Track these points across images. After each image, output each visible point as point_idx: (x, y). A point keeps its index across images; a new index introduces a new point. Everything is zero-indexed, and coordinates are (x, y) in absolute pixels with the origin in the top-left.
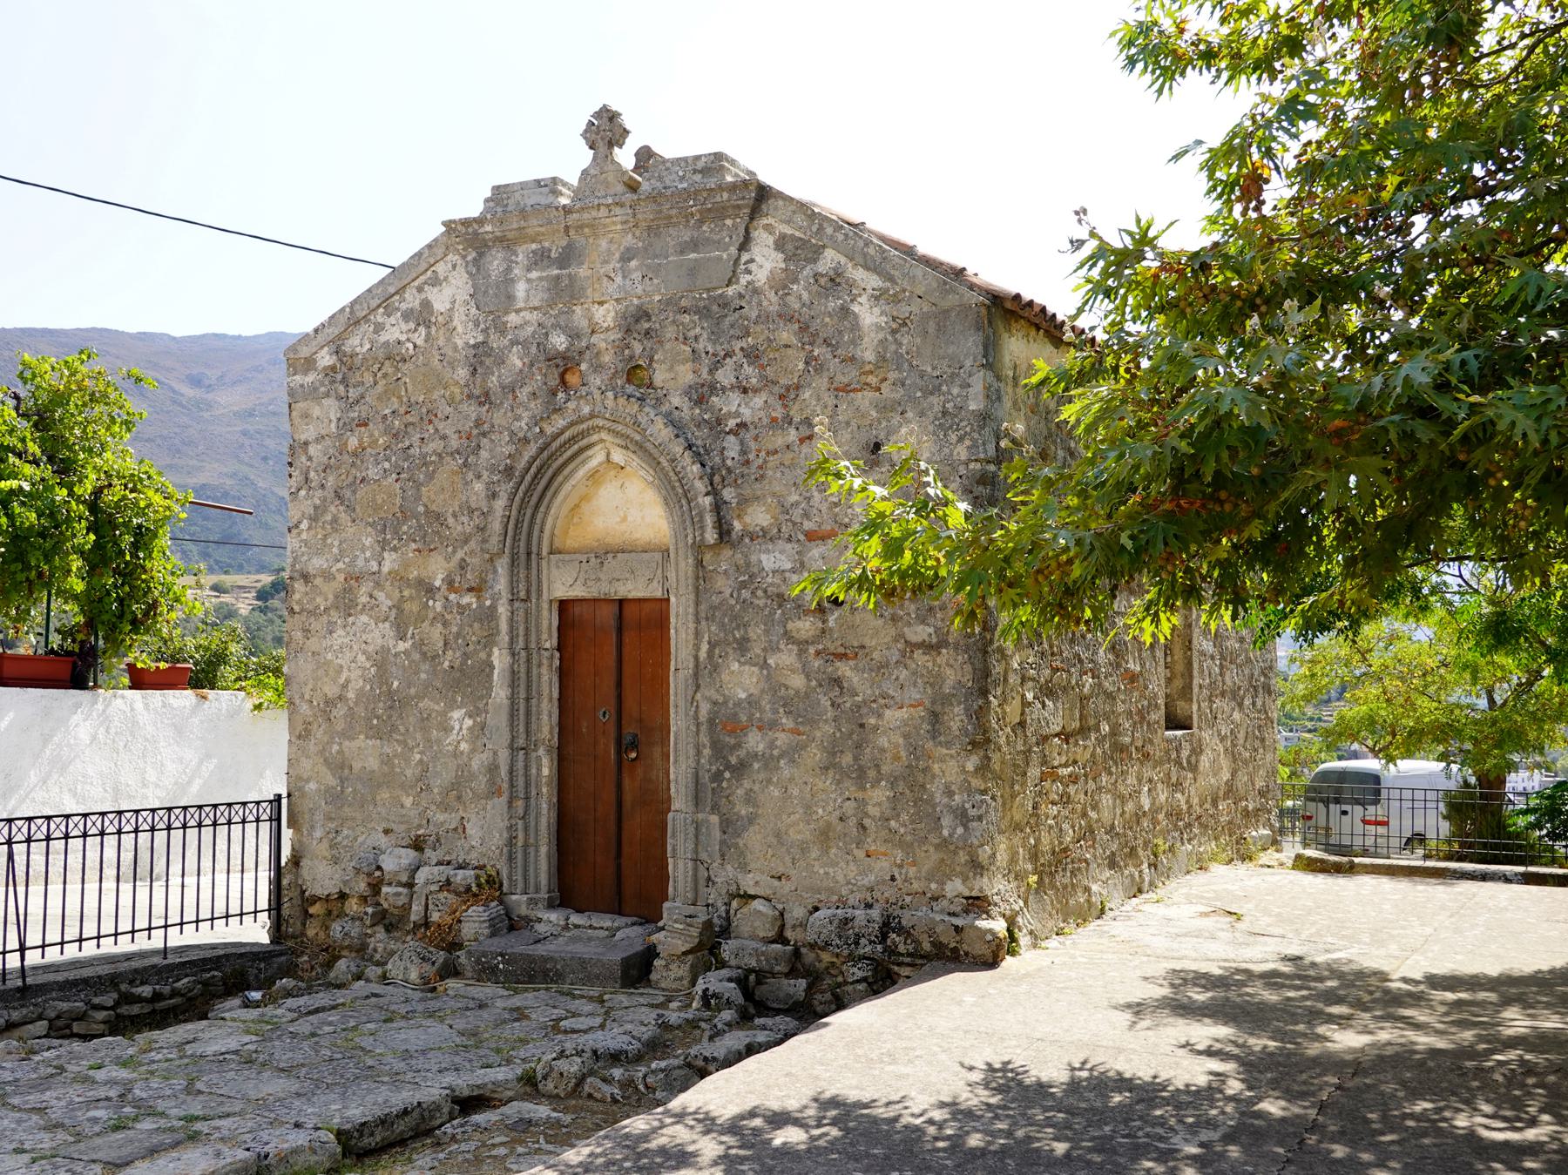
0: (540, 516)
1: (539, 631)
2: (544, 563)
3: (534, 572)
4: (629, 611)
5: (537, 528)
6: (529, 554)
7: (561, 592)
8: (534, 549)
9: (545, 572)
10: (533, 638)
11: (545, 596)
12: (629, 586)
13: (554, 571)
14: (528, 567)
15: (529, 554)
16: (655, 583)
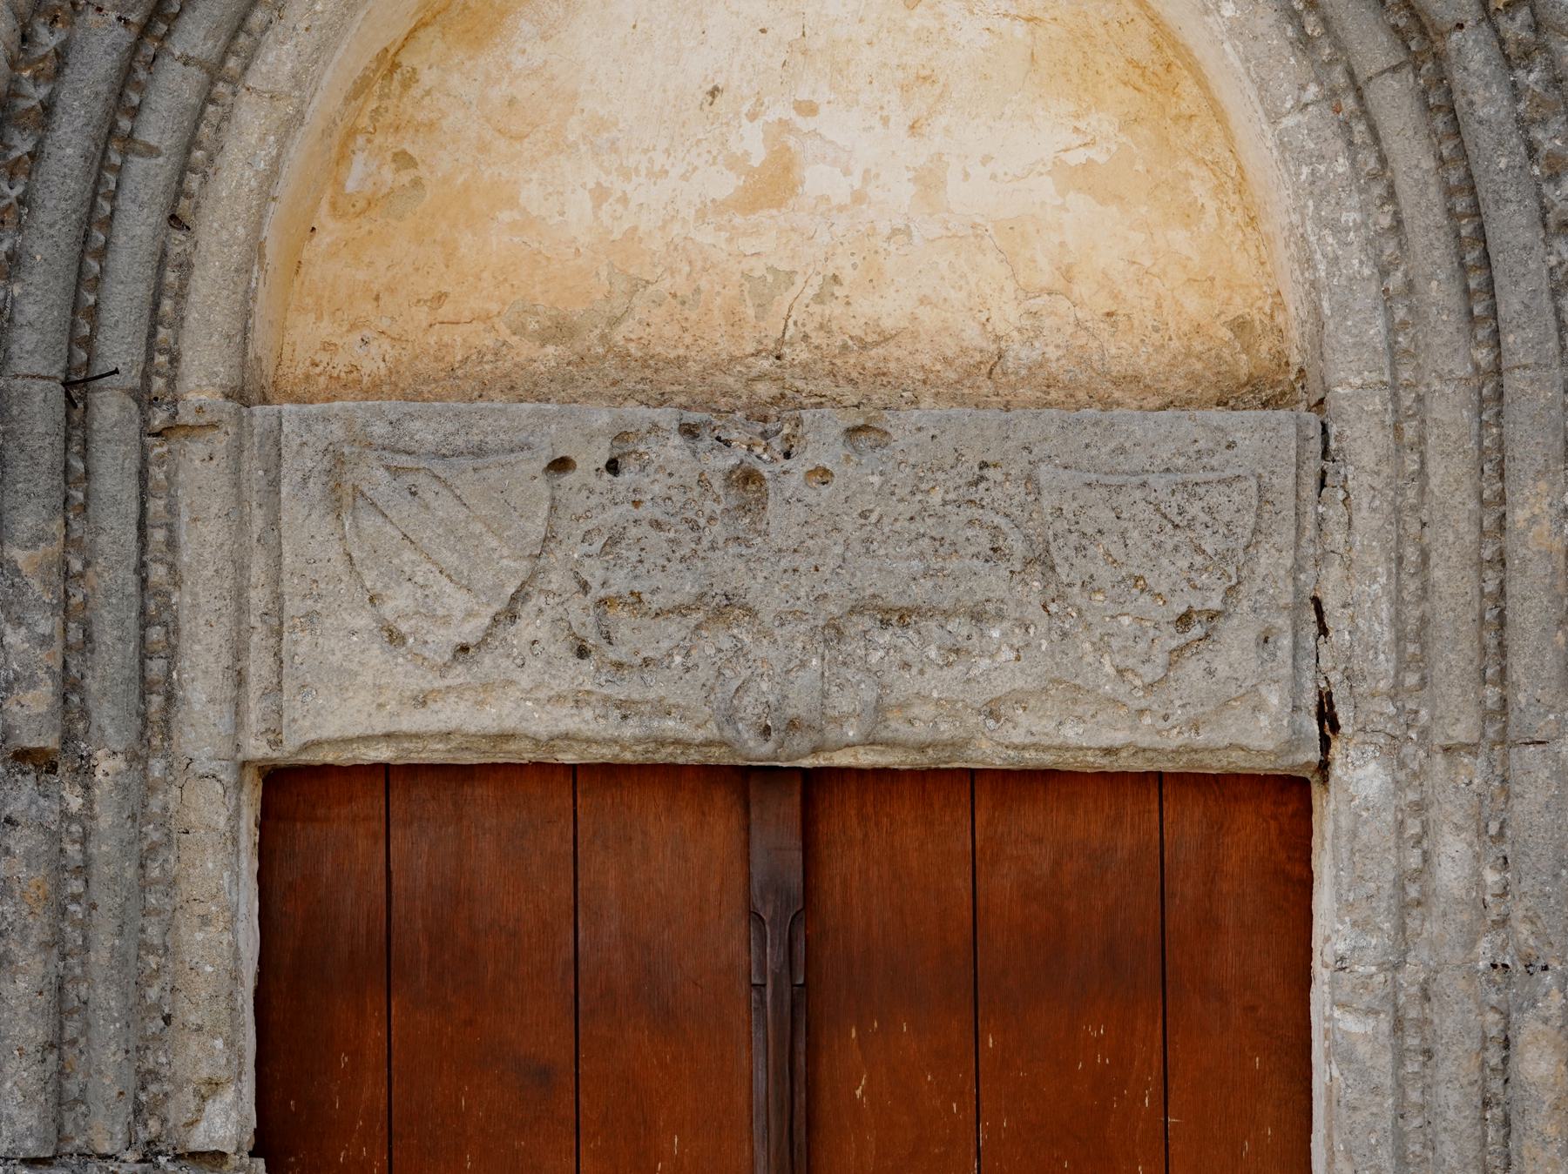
0: (173, 88)
1: (153, 1023)
2: (199, 471)
3: (114, 532)
4: (868, 866)
5: (145, 179)
6: (77, 387)
7: (355, 706)
8: (119, 348)
9: (203, 540)
10: (106, 1065)
11: (203, 727)
12: (1000, 663)
13: (307, 529)
14: (74, 493)
15: (77, 387)
16: (1234, 650)
